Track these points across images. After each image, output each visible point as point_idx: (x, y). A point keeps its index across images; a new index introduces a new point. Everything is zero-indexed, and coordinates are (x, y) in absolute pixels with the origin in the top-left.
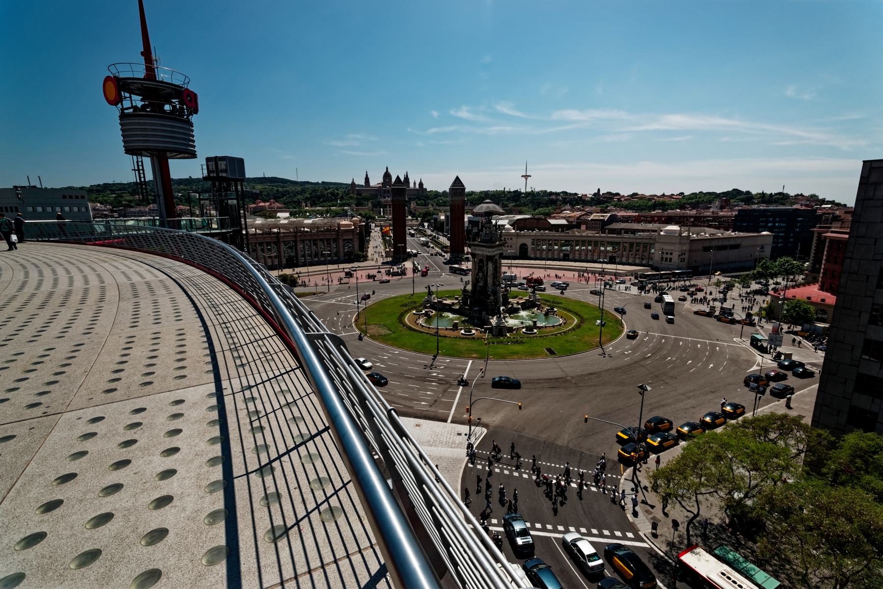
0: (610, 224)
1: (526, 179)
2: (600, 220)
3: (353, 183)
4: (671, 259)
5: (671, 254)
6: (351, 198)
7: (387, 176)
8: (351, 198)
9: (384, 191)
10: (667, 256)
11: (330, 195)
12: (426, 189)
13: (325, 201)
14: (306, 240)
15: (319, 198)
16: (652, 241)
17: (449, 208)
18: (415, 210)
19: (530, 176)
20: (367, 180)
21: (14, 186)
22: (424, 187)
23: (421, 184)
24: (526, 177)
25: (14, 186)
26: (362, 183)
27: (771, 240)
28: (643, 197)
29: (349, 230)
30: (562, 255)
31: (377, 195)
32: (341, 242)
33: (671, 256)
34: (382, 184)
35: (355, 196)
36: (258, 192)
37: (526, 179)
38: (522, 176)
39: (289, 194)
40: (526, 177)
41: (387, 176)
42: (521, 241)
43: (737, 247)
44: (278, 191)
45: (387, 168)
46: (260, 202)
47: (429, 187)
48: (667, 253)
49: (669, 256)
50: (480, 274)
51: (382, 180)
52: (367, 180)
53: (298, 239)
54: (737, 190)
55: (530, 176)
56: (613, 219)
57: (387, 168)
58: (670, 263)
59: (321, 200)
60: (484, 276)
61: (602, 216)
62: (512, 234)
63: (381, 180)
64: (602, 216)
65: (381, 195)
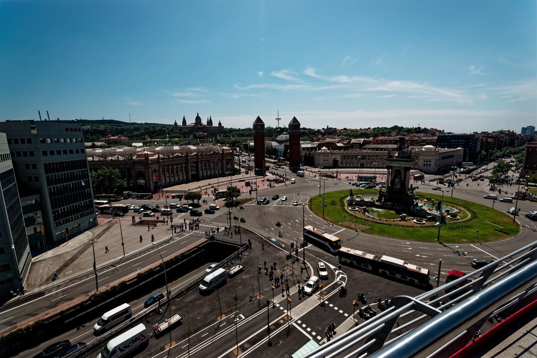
0: (364, 145)
1: (278, 121)
2: (358, 143)
3: (176, 124)
4: (430, 165)
5: (430, 161)
6: (176, 133)
7: (198, 119)
8: (176, 133)
9: (197, 128)
10: (427, 163)
11: (160, 131)
12: (223, 127)
13: (157, 135)
14: (204, 161)
15: (153, 133)
16: (416, 155)
17: (253, 138)
18: (222, 140)
19: (281, 119)
20: (184, 121)
21: (6, 121)
22: (222, 125)
23: (220, 124)
24: (278, 119)
25: (6, 121)
26: (180, 123)
27: (462, 153)
28: (352, 131)
29: (229, 153)
30: (359, 165)
31: (192, 131)
32: (225, 160)
33: (430, 163)
34: (195, 124)
35: (178, 132)
36: (103, 129)
37: (278, 121)
38: (276, 119)
39: (126, 131)
40: (278, 119)
41: (198, 119)
42: (334, 157)
43: (452, 156)
44: (117, 129)
45: (198, 114)
46: (110, 136)
47: (227, 125)
48: (427, 161)
49: (429, 163)
50: (397, 180)
51: (195, 121)
52: (184, 121)
53: (199, 160)
54: (397, 126)
55: (281, 119)
56: (365, 143)
57: (198, 114)
58: (430, 167)
59: (155, 134)
60: (401, 181)
61: (358, 141)
62: (328, 153)
63: (194, 121)
64: (358, 141)
65: (195, 131)
